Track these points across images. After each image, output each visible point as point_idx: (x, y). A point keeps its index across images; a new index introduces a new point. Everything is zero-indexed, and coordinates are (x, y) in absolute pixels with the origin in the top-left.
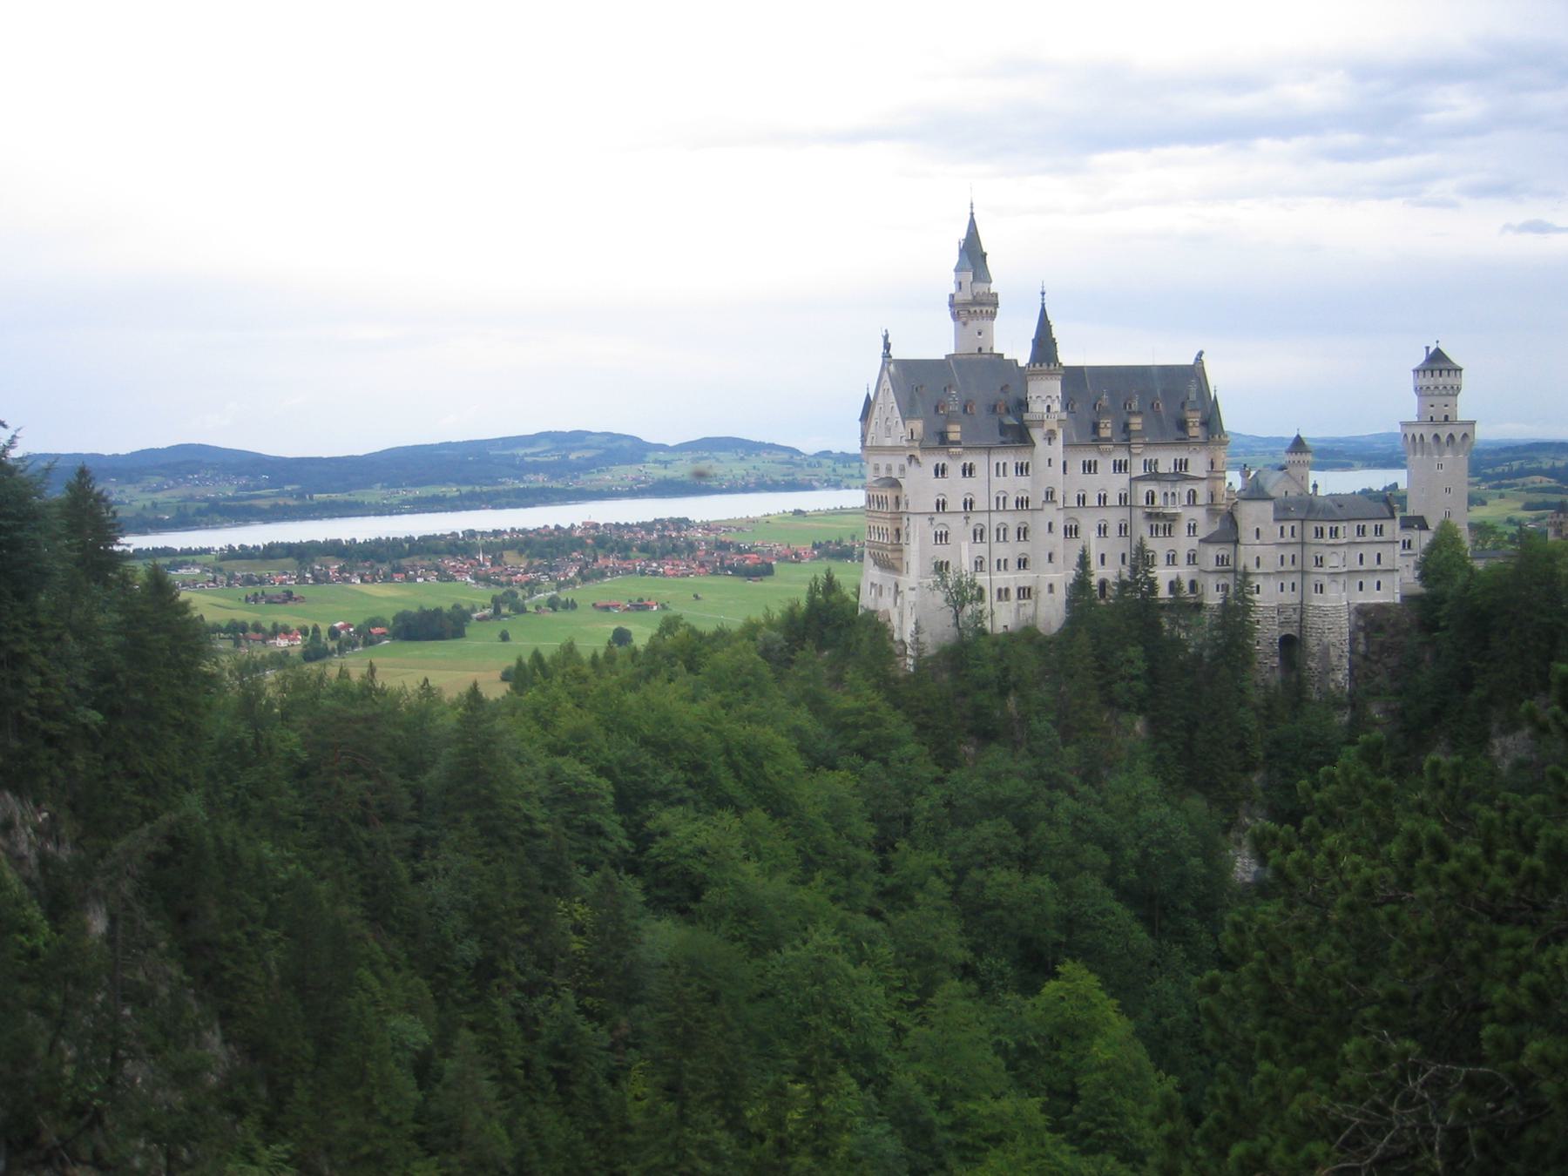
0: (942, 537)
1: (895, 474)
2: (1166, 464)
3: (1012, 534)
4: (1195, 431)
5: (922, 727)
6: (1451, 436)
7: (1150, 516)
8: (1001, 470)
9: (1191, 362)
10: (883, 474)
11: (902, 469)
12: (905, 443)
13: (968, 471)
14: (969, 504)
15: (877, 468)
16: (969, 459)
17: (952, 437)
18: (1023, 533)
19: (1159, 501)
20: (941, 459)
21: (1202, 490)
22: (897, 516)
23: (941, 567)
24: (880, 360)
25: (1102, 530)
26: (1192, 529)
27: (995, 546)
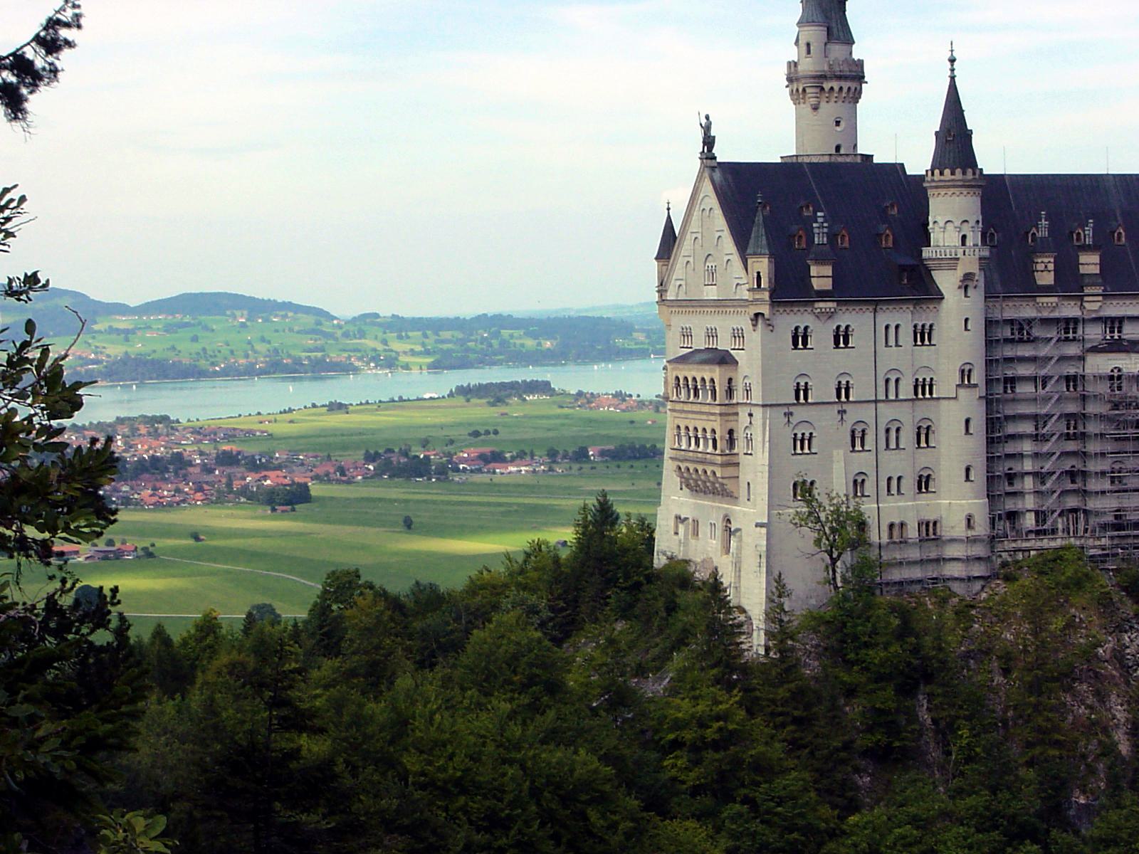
0: (802, 442)
1: (724, 344)
3: (907, 437)
5: (794, 745)
8: (891, 335)
10: (700, 343)
11: (738, 335)
12: (746, 295)
13: (842, 338)
14: (843, 390)
15: (687, 334)
16: (846, 318)
17: (817, 284)
18: (924, 434)
20: (802, 319)
22: (729, 410)
23: (804, 490)
24: (697, 164)
27: (884, 455)
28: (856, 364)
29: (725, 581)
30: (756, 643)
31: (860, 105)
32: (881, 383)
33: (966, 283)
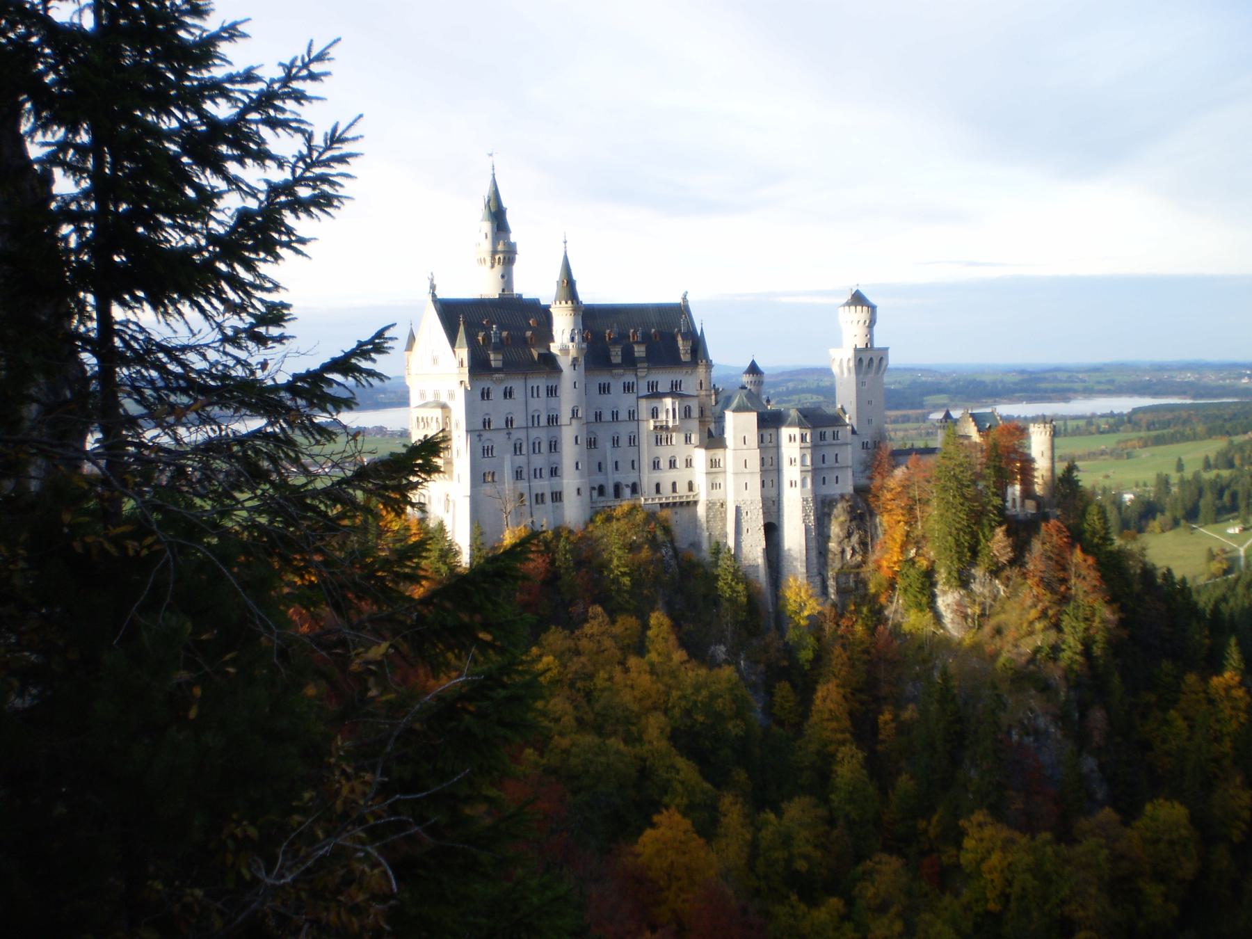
1: (444, 399)
2: (663, 387)
3: (544, 447)
4: (685, 357)
6: (871, 359)
7: (655, 427)
8: (535, 392)
9: (676, 299)
10: (430, 398)
11: (452, 395)
13: (508, 394)
14: (509, 422)
15: (422, 395)
18: (554, 446)
19: (662, 416)
20: (486, 383)
21: (694, 405)
25: (616, 442)
26: (688, 440)
28: (515, 408)
29: (448, 528)
30: (465, 559)
31: (517, 268)
32: (530, 418)
33: (575, 362)
